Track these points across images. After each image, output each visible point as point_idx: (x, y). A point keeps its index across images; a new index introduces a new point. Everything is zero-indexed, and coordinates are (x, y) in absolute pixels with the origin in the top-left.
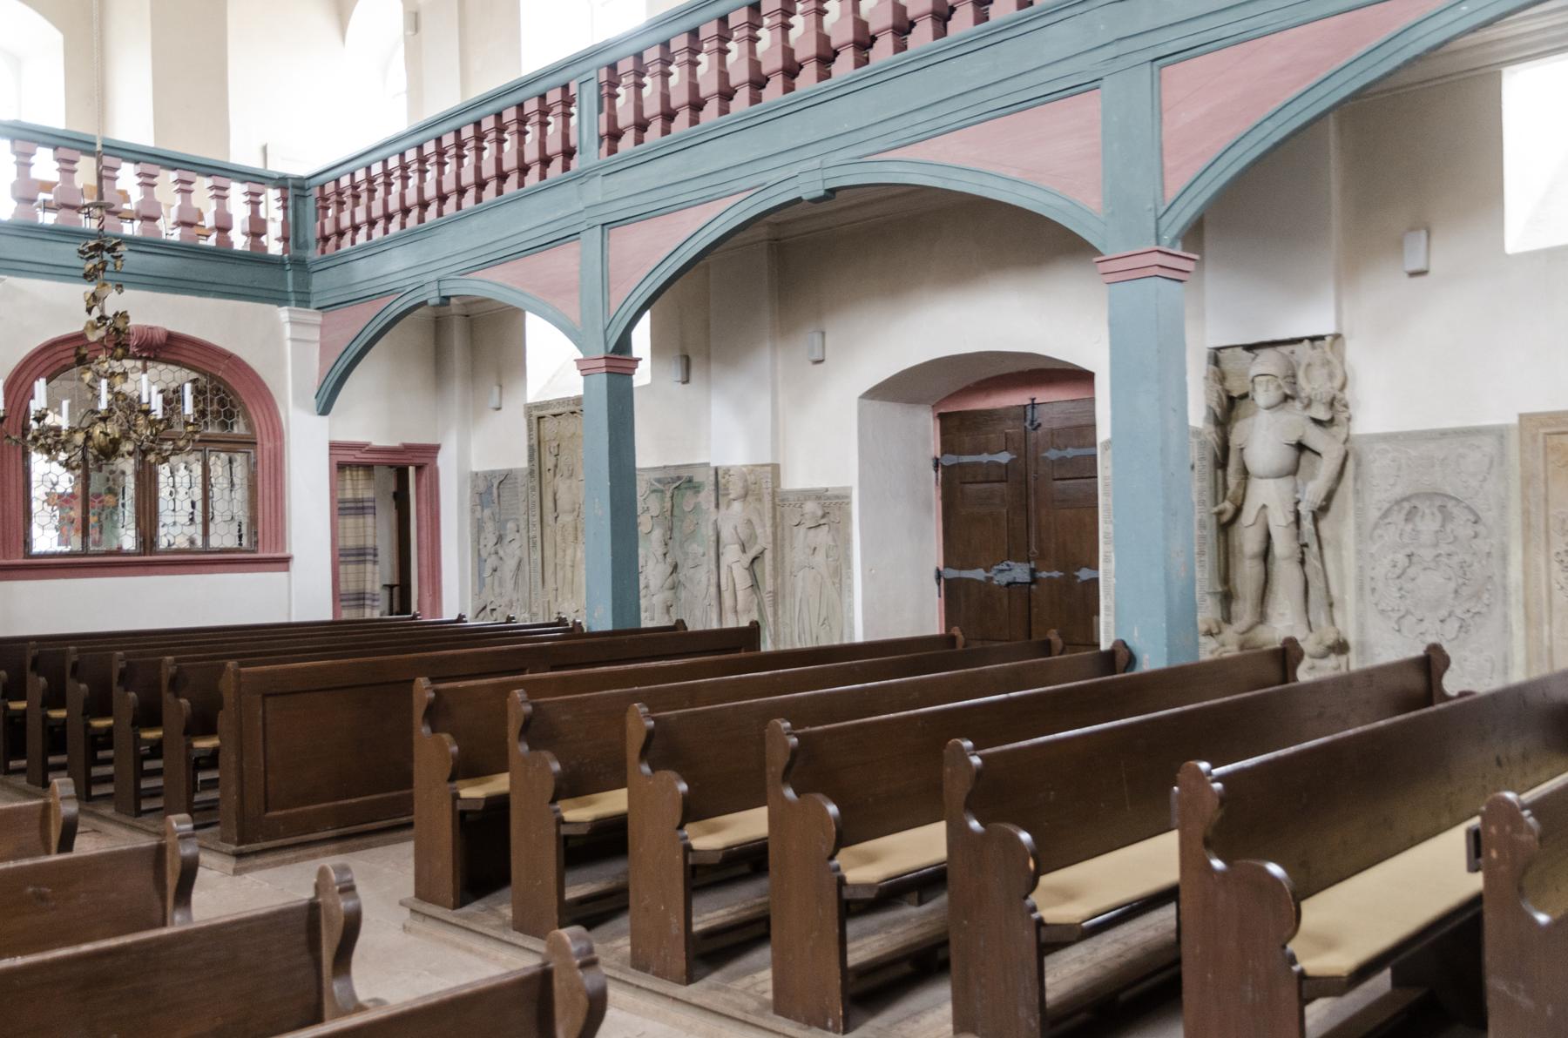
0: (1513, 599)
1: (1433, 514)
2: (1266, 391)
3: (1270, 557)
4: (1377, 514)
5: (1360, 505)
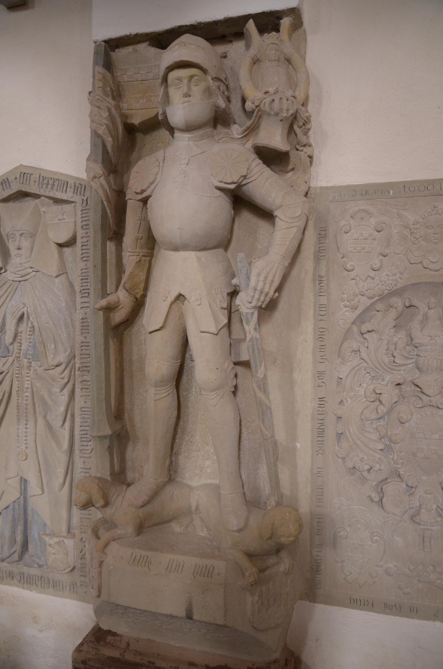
2: (187, 95)
3: (185, 379)
4: (351, 316)
5: (323, 300)
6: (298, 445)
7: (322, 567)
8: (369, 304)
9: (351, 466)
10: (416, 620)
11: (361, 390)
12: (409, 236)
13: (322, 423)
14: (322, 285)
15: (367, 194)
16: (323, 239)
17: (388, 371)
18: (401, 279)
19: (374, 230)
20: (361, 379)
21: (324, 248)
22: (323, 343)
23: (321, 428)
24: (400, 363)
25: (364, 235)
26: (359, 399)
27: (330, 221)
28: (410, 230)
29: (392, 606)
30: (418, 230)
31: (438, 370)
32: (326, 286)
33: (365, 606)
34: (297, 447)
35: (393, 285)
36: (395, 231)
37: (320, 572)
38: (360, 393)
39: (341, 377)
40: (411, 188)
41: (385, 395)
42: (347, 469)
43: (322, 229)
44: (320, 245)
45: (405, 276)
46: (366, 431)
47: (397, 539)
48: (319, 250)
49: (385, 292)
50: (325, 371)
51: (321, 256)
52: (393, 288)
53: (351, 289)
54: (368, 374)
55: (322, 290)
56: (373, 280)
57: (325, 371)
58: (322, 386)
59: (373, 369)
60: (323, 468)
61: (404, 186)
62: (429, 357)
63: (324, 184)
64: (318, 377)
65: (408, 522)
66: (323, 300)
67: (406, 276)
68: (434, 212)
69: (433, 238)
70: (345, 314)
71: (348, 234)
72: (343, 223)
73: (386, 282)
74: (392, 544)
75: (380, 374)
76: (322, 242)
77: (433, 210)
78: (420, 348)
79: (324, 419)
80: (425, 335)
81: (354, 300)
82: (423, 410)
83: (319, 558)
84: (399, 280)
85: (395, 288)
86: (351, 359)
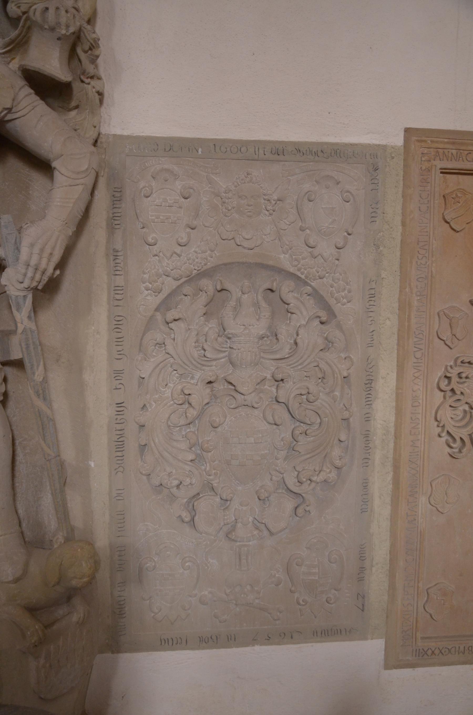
0: (378, 456)
1: (256, 305)
5: (120, 281)
6: (92, 464)
7: (126, 609)
8: (174, 287)
9: (158, 484)
10: (234, 648)
11: (168, 391)
12: (220, 206)
13: (121, 434)
14: (117, 261)
15: (171, 150)
16: (118, 202)
17: (197, 367)
18: (212, 257)
19: (180, 196)
20: (167, 378)
21: (119, 215)
22: (120, 335)
23: (119, 440)
24: (211, 357)
25: (169, 201)
26: (165, 402)
27: (127, 180)
28: (222, 199)
29: (208, 639)
30: (230, 200)
31: (252, 365)
32: (122, 263)
33: (178, 644)
34: (90, 466)
35: (202, 264)
36: (205, 199)
37: (124, 615)
38: (166, 395)
39: (143, 376)
40: (222, 148)
41: (195, 396)
42: (152, 488)
43: (116, 190)
44: (115, 210)
45: (216, 255)
46: (175, 440)
47: (211, 561)
48: (113, 217)
49: (193, 273)
50: (123, 370)
51: (115, 225)
52: (202, 267)
53: (153, 267)
54: (175, 372)
55: (118, 268)
56: (180, 257)
57: (123, 370)
58: (120, 389)
59: (181, 366)
60: (124, 489)
61: (215, 145)
62: (242, 349)
63: (118, 132)
64: (115, 377)
65: (223, 540)
66: (120, 281)
67: (217, 254)
68: (248, 179)
69: (246, 211)
70: (146, 299)
71: (149, 199)
72: (142, 184)
73: (194, 260)
74: (206, 568)
75: (189, 371)
76: (117, 206)
77: (246, 177)
78: (233, 339)
79: (124, 429)
80: (239, 324)
81: (157, 282)
82: (237, 410)
83: (123, 598)
84: (209, 258)
85: (205, 268)
86: (154, 354)
